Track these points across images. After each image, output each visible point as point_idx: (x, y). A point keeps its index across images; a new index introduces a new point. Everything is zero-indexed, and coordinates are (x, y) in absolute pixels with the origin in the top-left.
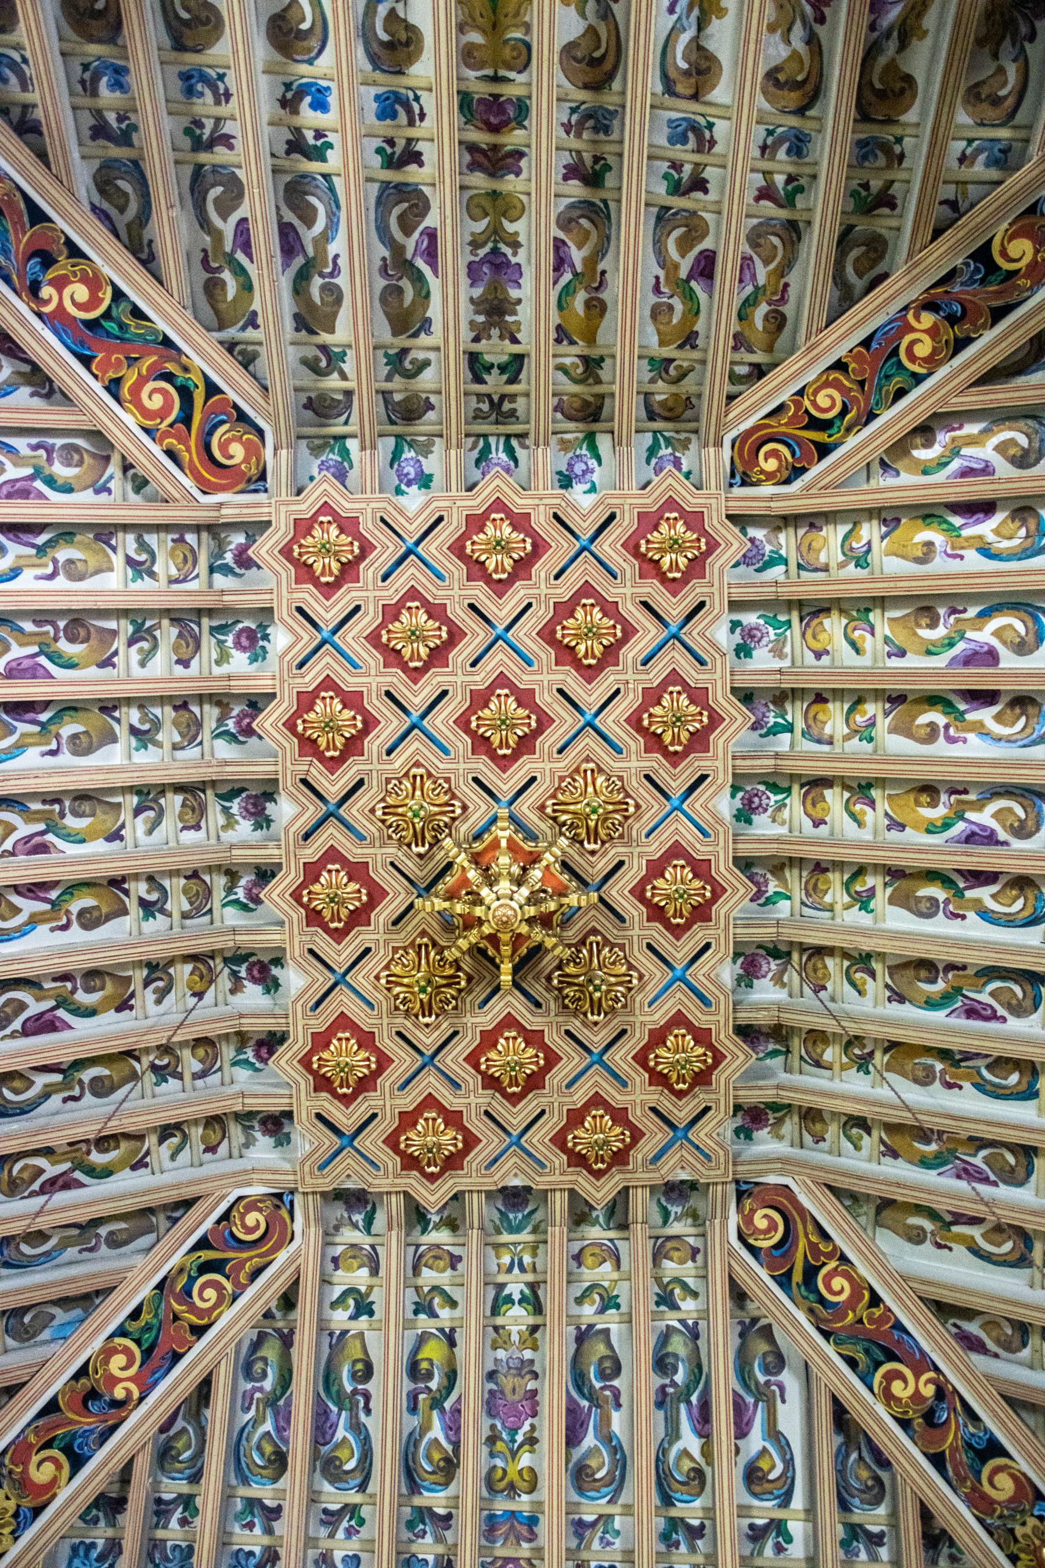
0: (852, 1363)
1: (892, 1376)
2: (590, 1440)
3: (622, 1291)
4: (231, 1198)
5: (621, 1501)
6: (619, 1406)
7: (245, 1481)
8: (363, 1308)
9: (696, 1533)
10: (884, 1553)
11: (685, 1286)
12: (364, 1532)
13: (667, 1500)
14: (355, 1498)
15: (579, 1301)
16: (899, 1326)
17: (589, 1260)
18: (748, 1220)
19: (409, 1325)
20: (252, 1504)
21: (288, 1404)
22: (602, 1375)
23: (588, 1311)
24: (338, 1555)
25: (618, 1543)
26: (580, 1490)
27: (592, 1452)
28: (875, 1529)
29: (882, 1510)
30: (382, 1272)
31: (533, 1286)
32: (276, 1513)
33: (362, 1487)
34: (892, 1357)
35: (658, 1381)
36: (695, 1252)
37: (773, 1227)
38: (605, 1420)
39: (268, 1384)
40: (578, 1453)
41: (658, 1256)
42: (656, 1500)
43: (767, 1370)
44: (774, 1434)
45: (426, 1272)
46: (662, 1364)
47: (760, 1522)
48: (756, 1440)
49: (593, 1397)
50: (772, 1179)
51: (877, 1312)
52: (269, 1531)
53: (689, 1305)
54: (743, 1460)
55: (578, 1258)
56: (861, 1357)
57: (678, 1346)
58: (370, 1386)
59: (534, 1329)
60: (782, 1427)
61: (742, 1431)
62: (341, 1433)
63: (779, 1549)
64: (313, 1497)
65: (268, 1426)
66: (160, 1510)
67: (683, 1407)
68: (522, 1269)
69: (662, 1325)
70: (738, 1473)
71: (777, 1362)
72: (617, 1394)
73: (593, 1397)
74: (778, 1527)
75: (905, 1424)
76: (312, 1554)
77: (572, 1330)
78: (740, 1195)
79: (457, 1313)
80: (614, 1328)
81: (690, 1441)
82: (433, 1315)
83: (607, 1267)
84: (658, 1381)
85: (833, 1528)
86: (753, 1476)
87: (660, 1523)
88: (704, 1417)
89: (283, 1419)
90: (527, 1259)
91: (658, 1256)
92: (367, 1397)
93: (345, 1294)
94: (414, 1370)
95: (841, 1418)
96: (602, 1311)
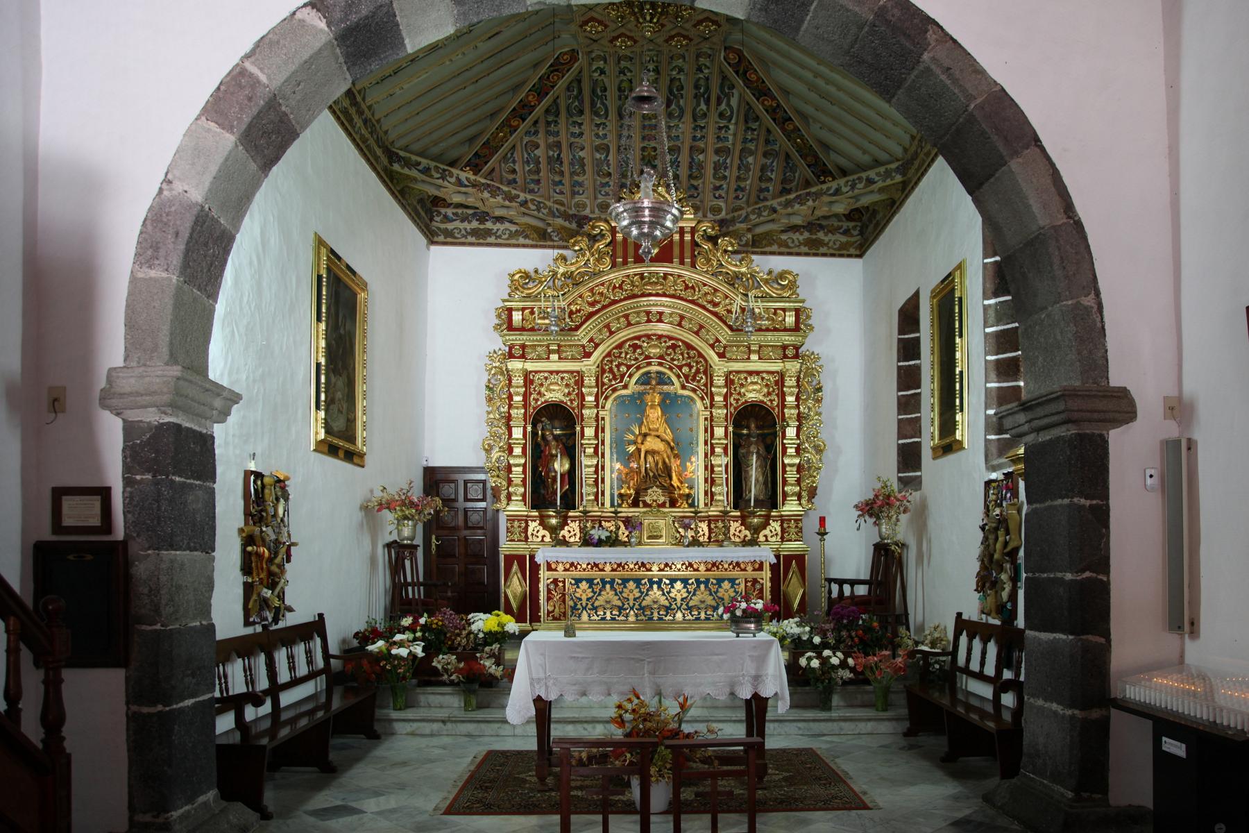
0: (754, 95)
1: (764, 100)
2: (673, 106)
3: (686, 67)
4: (558, 53)
5: (682, 120)
6: (682, 98)
7: (572, 117)
8: (602, 72)
9: (704, 127)
10: (756, 133)
11: (705, 65)
12: (607, 129)
13: (695, 120)
14: (604, 121)
15: (672, 70)
16: (769, 89)
17: (675, 58)
18: (728, 55)
19: (617, 77)
20: (574, 122)
21: (582, 98)
22: (678, 90)
23: (674, 73)
24: (601, 134)
25: (680, 130)
26: (670, 118)
27: (674, 109)
28: (754, 127)
29: (757, 123)
30: (608, 62)
31: (657, 67)
32: (582, 124)
33: (606, 118)
34: (766, 95)
35: (694, 91)
36: (710, 56)
37: (735, 58)
38: (679, 102)
39: (575, 93)
40: (669, 110)
41: (698, 56)
42: (692, 120)
43: (729, 89)
44: (728, 105)
45: (622, 62)
46: (697, 87)
47: (722, 125)
48: (723, 106)
49: (675, 96)
50: (736, 47)
51: (763, 85)
52: (580, 128)
53: (706, 71)
54: (718, 111)
55: (672, 58)
56: (757, 94)
57: (702, 82)
58: (607, 93)
59: (657, 79)
60: (732, 103)
61: (719, 102)
62: (598, 105)
63: (726, 131)
64: (592, 120)
65: (577, 103)
66: (548, 123)
67: (702, 99)
68: (653, 61)
69: (697, 76)
70: (717, 115)
71: (732, 87)
72: (682, 95)
73: (675, 96)
74: (727, 127)
75: (767, 111)
76: (593, 133)
77: (668, 79)
78: (726, 48)
79: (633, 74)
80: (682, 77)
81: (703, 107)
82: (625, 75)
83: (681, 60)
84: (694, 91)
85: (742, 127)
86: (721, 115)
87: (693, 126)
88: (707, 102)
89: (581, 102)
90: (655, 59)
91: (698, 56)
92: (606, 96)
93: (598, 68)
94: (620, 89)
95: (748, 104)
96: (678, 73)
